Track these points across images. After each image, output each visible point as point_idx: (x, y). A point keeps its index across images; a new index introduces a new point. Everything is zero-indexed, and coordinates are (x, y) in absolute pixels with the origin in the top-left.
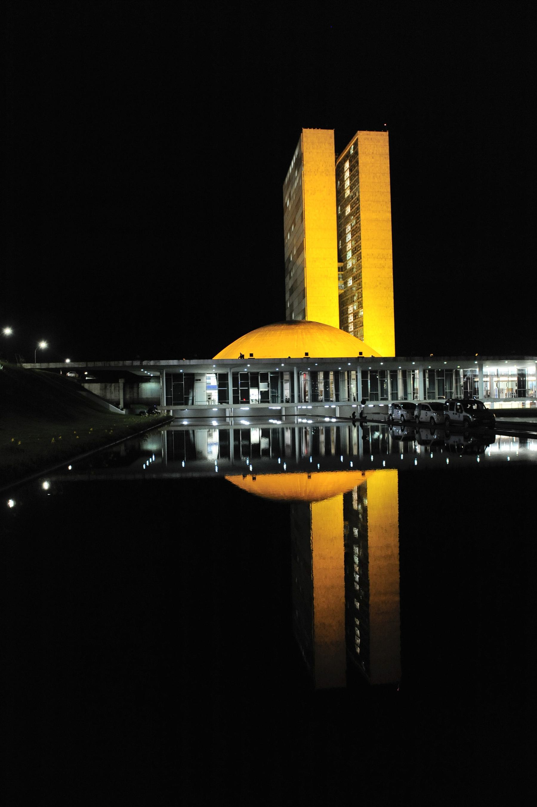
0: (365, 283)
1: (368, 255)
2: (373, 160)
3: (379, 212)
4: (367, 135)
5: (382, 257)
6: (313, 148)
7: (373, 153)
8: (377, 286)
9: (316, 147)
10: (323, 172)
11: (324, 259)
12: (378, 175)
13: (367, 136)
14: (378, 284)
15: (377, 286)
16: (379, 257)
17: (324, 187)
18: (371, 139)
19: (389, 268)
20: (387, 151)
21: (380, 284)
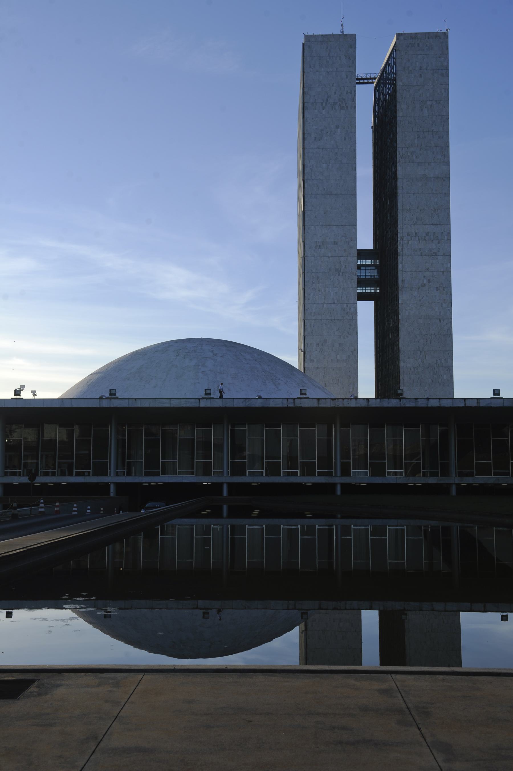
1: (409, 235)
3: (429, 164)
5: (432, 238)
7: (421, 68)
11: (335, 243)
12: (429, 103)
15: (423, 285)
16: (427, 238)
17: (337, 127)
18: (418, 45)
19: (444, 255)
21: (429, 281)
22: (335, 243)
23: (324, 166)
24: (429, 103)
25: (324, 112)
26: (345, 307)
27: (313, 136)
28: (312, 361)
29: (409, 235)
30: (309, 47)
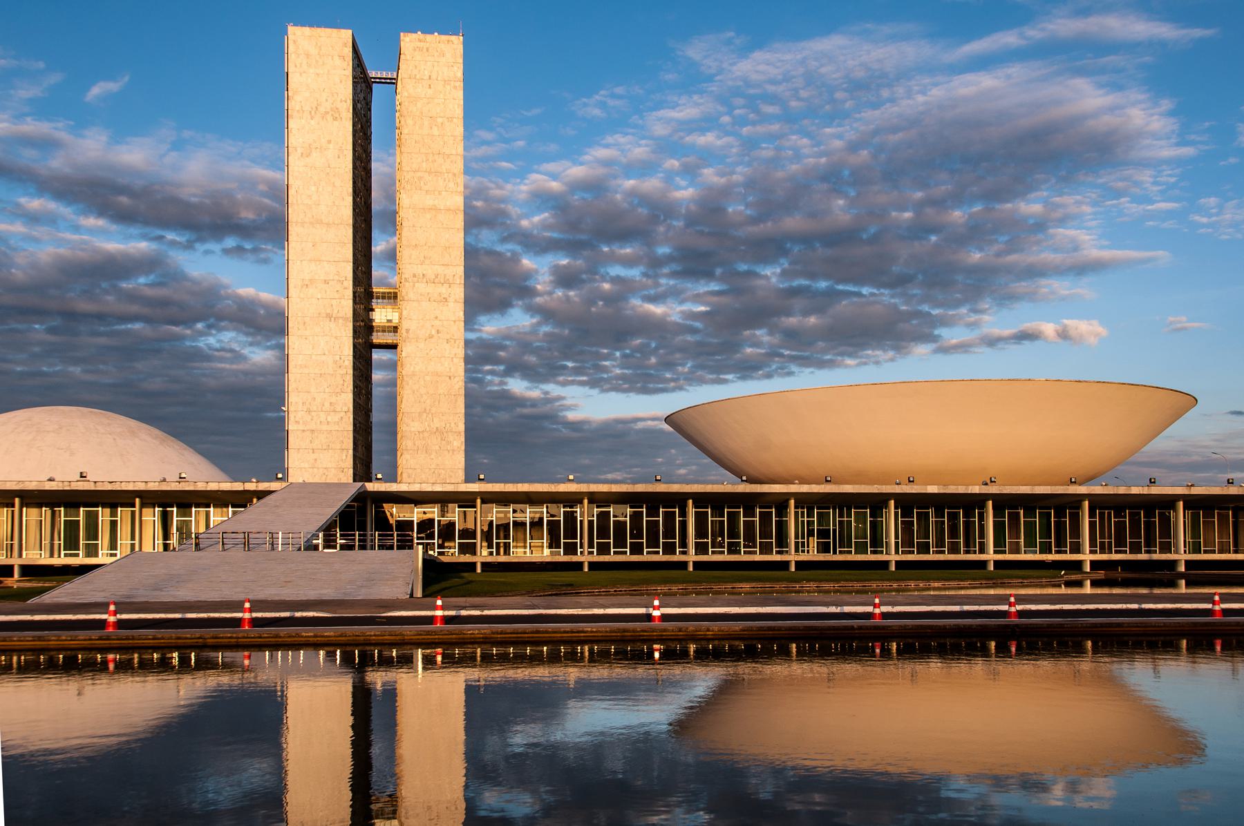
0: (408, 331)
1: (414, 276)
2: (430, 92)
3: (440, 193)
4: (420, 41)
6: (309, 65)
8: (431, 337)
9: (317, 62)
10: (327, 113)
11: (326, 282)
13: (419, 44)
14: (434, 332)
15: (431, 337)
17: (329, 142)
19: (456, 301)
20: (460, 74)
21: (438, 332)
22: (326, 282)
23: (313, 188)
24: (440, 120)
25: (313, 122)
26: (337, 358)
27: (299, 151)
28: (297, 422)
29: (414, 276)
30: (295, 42)
